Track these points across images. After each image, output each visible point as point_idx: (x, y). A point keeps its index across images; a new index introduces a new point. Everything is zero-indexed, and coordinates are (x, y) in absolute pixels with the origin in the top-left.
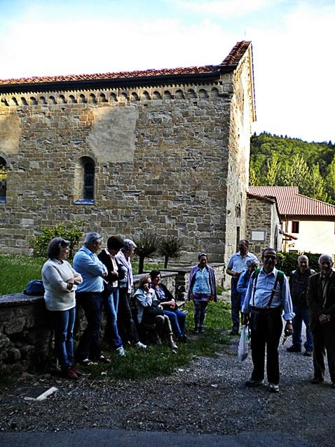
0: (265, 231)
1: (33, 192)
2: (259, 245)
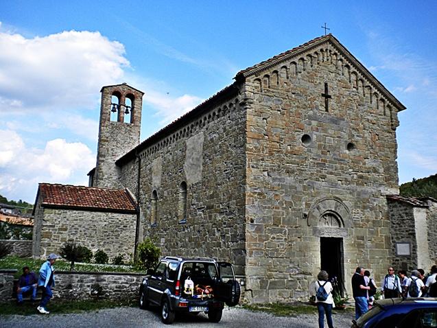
0: (409, 243)
1: (165, 216)
2: (405, 261)
